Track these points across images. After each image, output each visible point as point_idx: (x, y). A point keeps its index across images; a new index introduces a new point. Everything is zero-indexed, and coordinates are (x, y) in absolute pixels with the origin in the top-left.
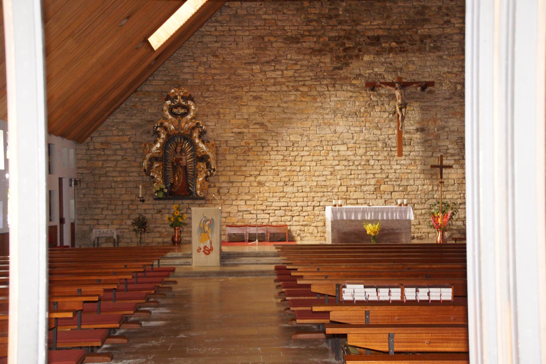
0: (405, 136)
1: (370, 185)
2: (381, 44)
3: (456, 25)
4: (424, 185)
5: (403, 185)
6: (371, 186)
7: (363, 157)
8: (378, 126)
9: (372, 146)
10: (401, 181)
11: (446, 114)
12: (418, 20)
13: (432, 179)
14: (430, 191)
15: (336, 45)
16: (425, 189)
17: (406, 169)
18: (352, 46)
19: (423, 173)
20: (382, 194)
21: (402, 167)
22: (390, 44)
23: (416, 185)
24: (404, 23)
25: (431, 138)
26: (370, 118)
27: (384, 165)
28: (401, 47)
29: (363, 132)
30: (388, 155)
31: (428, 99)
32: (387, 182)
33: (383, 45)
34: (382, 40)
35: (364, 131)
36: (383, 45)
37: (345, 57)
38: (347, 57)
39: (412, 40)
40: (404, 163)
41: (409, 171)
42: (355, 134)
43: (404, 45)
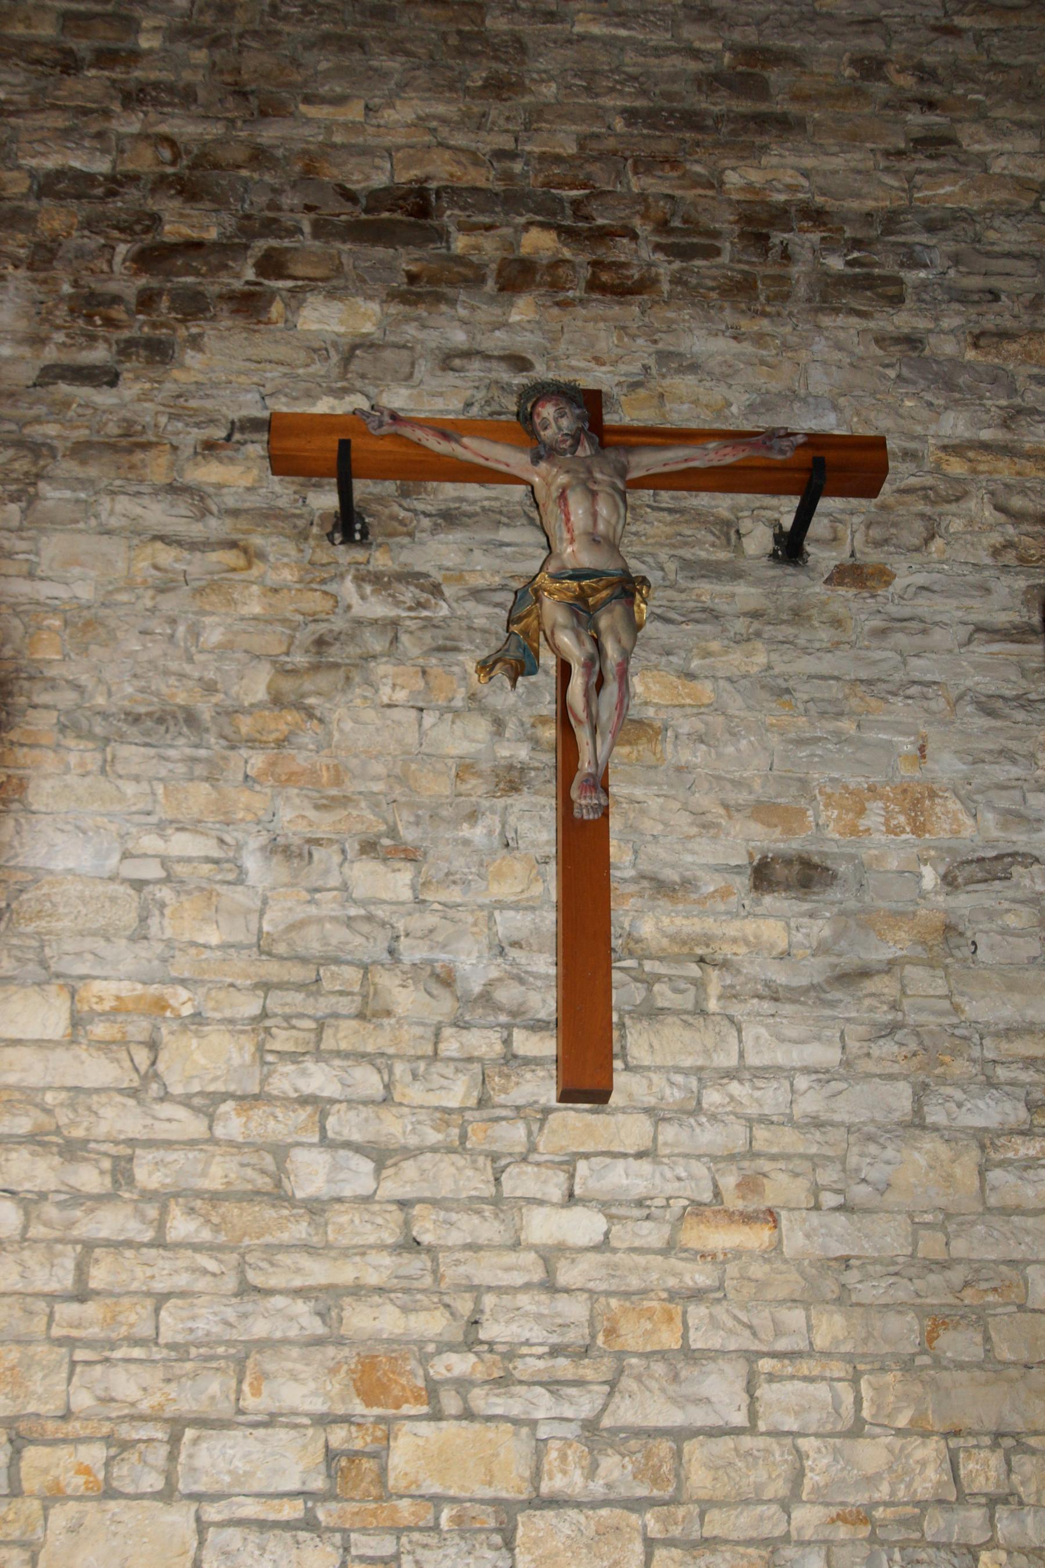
0: (647, 929)
1: (271, 1421)
2: (442, 235)
3: (998, 166)
4: (856, 1430)
5: (638, 1432)
6: (281, 1435)
7: (228, 1106)
8: (393, 832)
9: (323, 1006)
10: (613, 1384)
11: (1006, 755)
12: (719, 118)
13: (937, 1363)
14: (922, 1505)
15: (90, 225)
16: (870, 1481)
17: (669, 1249)
18: (212, 234)
19: (843, 1299)
20: (398, 1531)
21: (622, 1237)
22: (512, 245)
23: (775, 1434)
24: (619, 125)
25: (887, 953)
26: (323, 760)
27: (435, 1203)
28: (595, 264)
29: (240, 881)
30: (483, 1103)
31: (836, 623)
32: (463, 1385)
33: (460, 243)
34: (449, 216)
35: (252, 863)
36: (460, 243)
37: (147, 300)
38: (165, 303)
39: (676, 223)
40: (639, 1188)
41: (700, 1276)
42: (165, 893)
43: (622, 250)
